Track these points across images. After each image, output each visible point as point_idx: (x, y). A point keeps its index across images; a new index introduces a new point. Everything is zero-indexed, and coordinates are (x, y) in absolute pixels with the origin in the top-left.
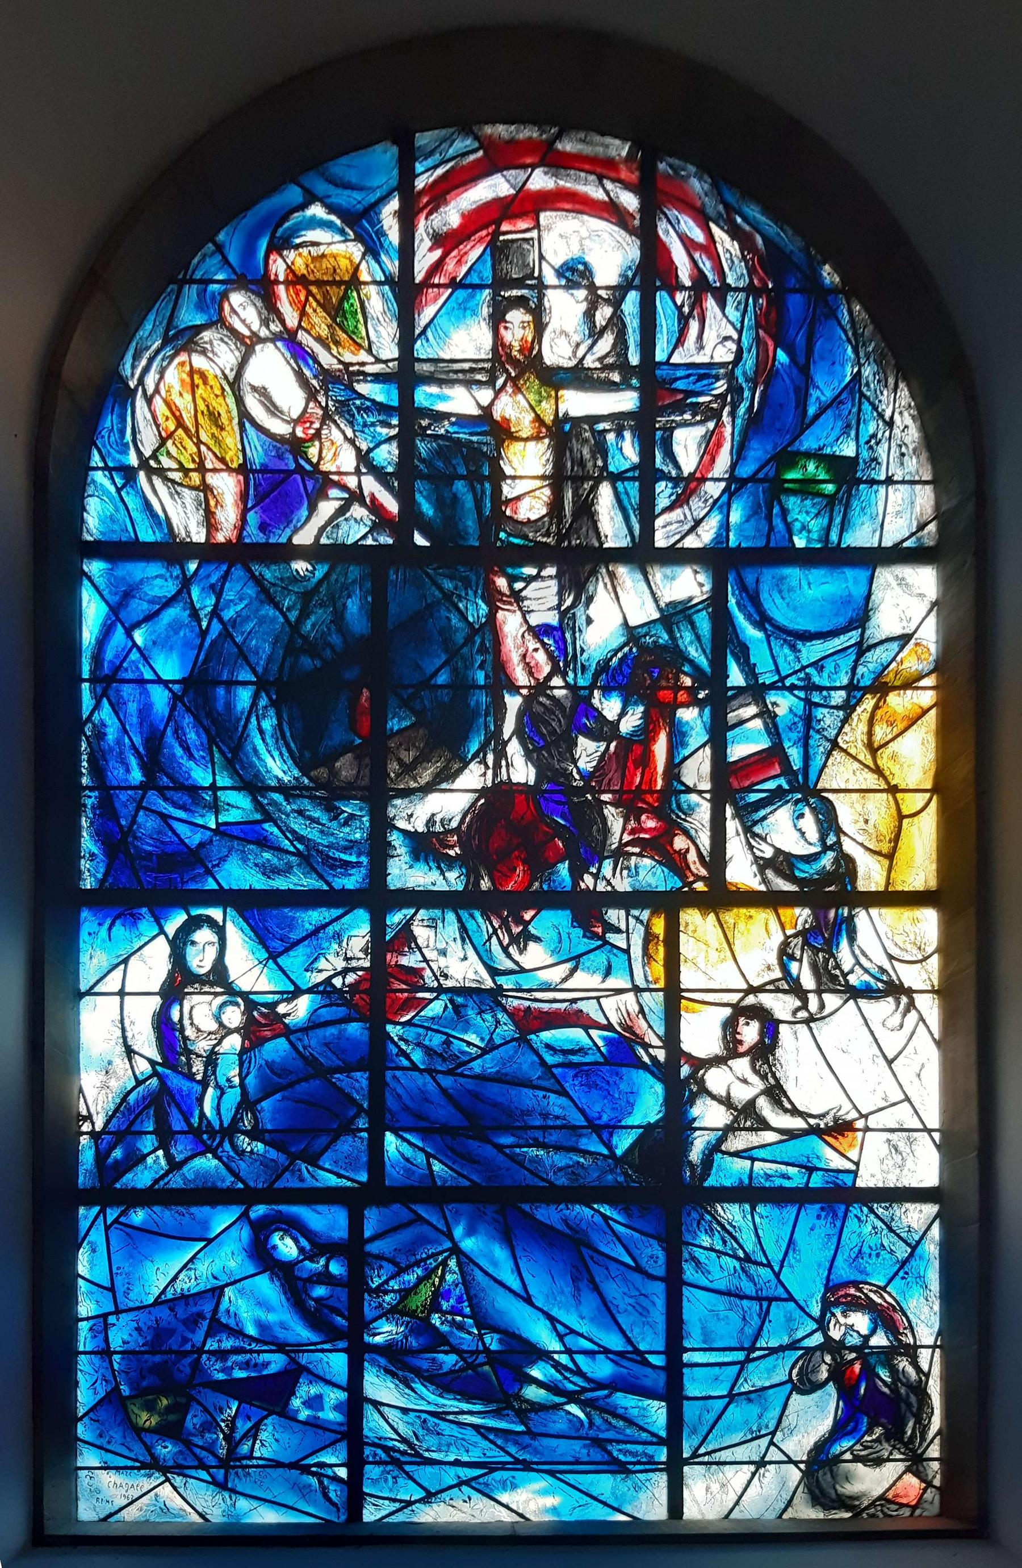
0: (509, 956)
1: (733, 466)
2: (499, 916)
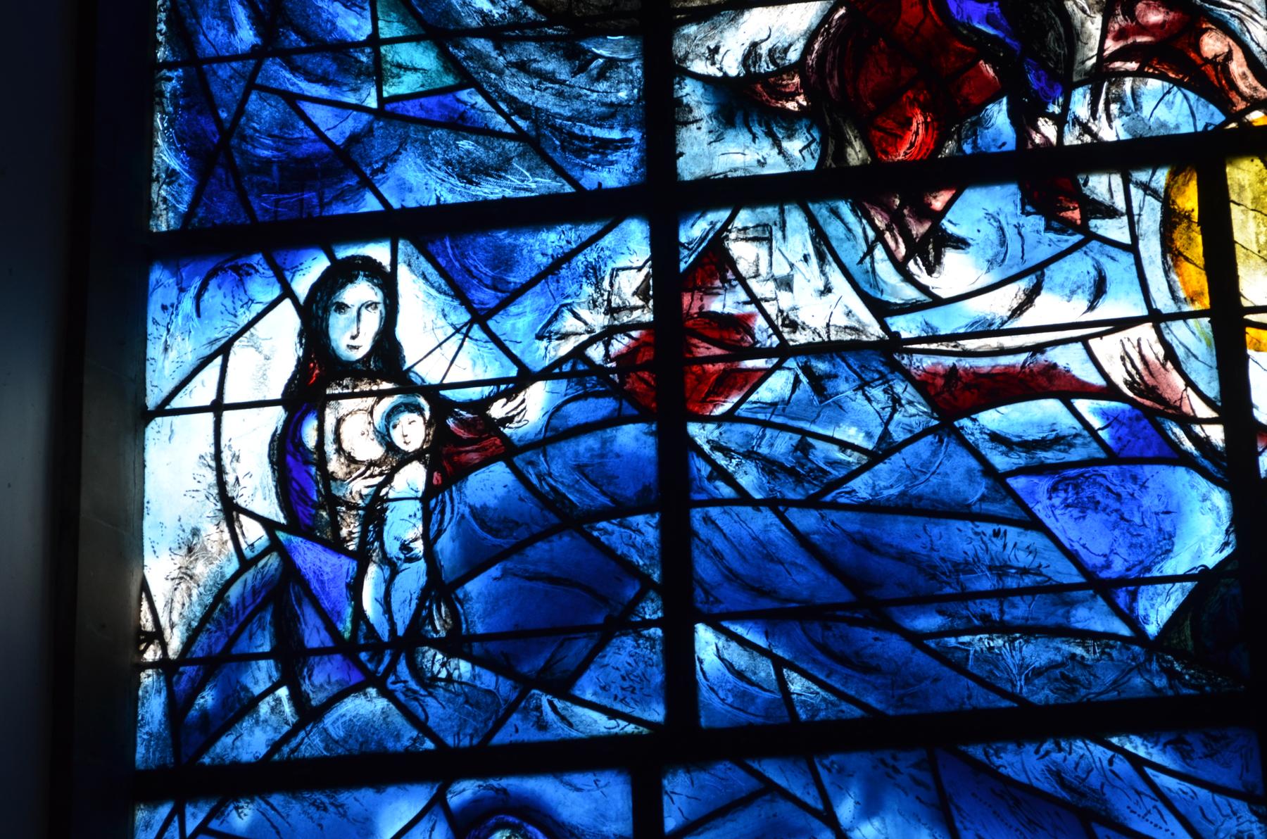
0: (909, 278)
2: (886, 208)
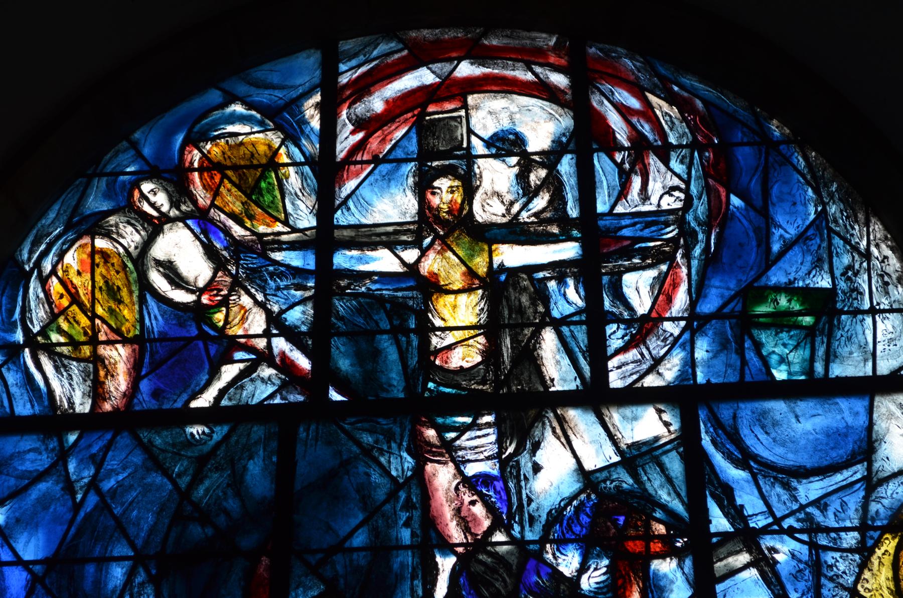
1: (693, 304)
